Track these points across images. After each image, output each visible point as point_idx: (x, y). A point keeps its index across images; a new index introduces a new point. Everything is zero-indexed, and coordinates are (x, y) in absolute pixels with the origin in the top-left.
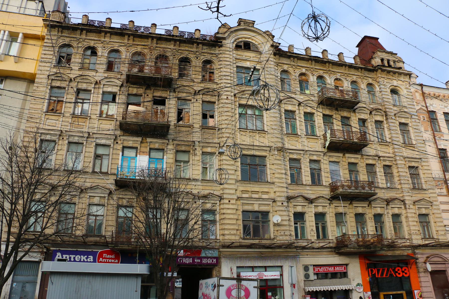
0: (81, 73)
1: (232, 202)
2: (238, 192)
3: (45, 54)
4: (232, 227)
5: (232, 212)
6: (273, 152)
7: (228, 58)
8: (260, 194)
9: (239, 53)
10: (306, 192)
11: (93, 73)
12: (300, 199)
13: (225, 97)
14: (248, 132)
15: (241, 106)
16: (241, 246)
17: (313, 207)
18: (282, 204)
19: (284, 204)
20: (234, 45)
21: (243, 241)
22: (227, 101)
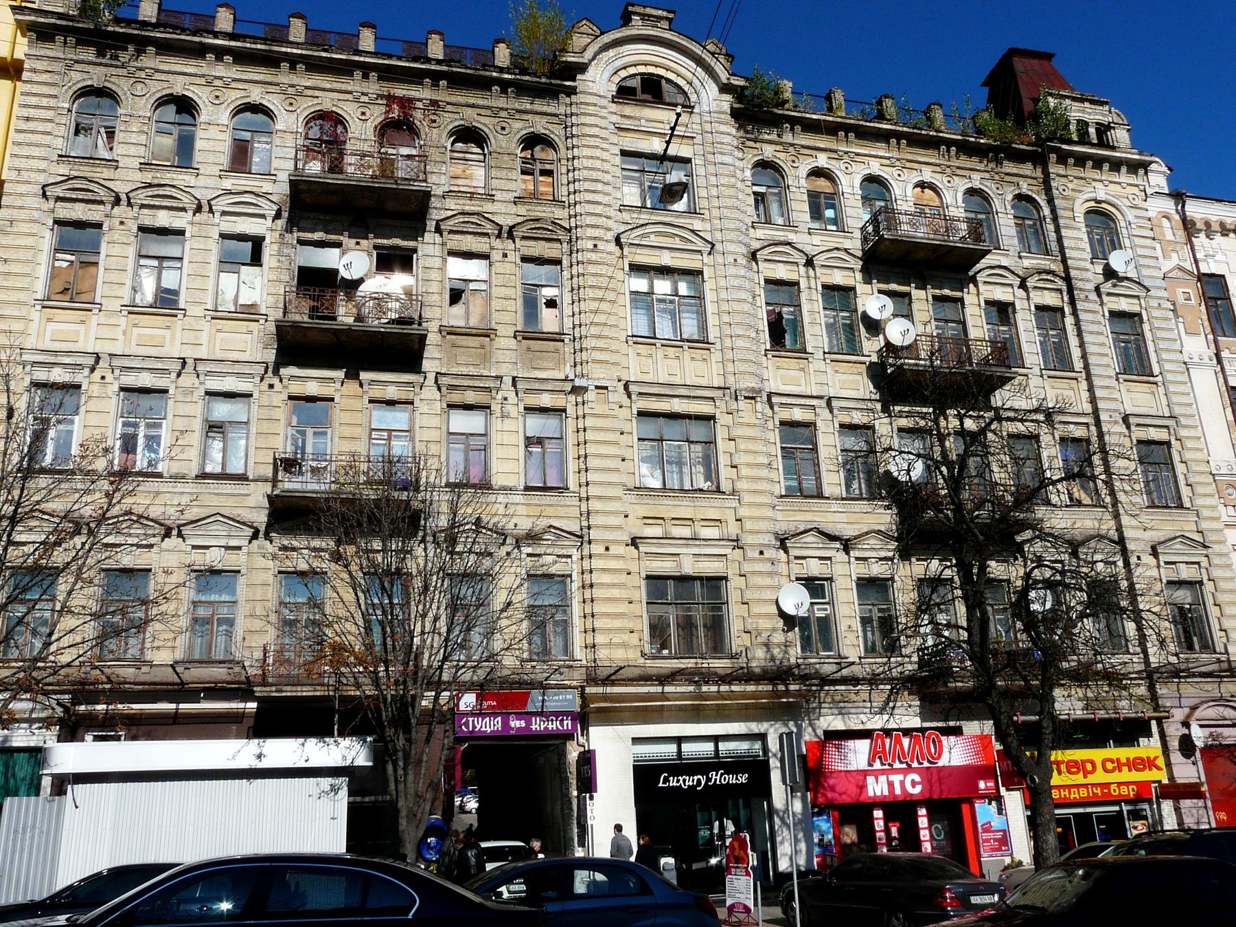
0: (148, 177)
1: (614, 550)
3: (28, 119)
4: (617, 623)
5: (615, 581)
9: (629, 110)
10: (830, 517)
11: (187, 177)
13: (590, 245)
15: (637, 269)
16: (645, 679)
18: (761, 553)
21: (649, 663)
22: (593, 256)
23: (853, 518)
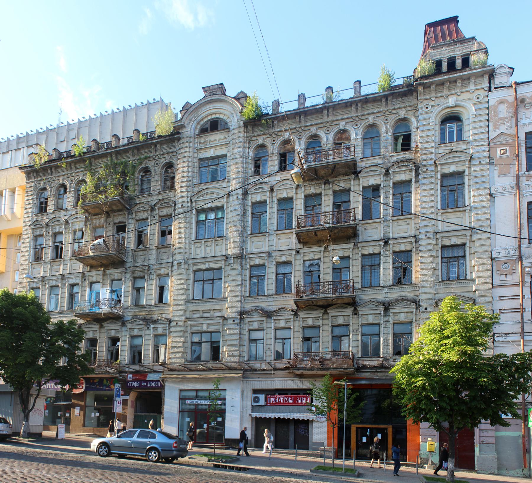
2: (188, 313)
6: (228, 262)
7: (186, 152)
8: (212, 313)
10: (266, 304)
12: (255, 314)
14: (203, 242)
15: (199, 211)
17: (273, 321)
19: (236, 322)
20: (197, 131)
23: (276, 303)
